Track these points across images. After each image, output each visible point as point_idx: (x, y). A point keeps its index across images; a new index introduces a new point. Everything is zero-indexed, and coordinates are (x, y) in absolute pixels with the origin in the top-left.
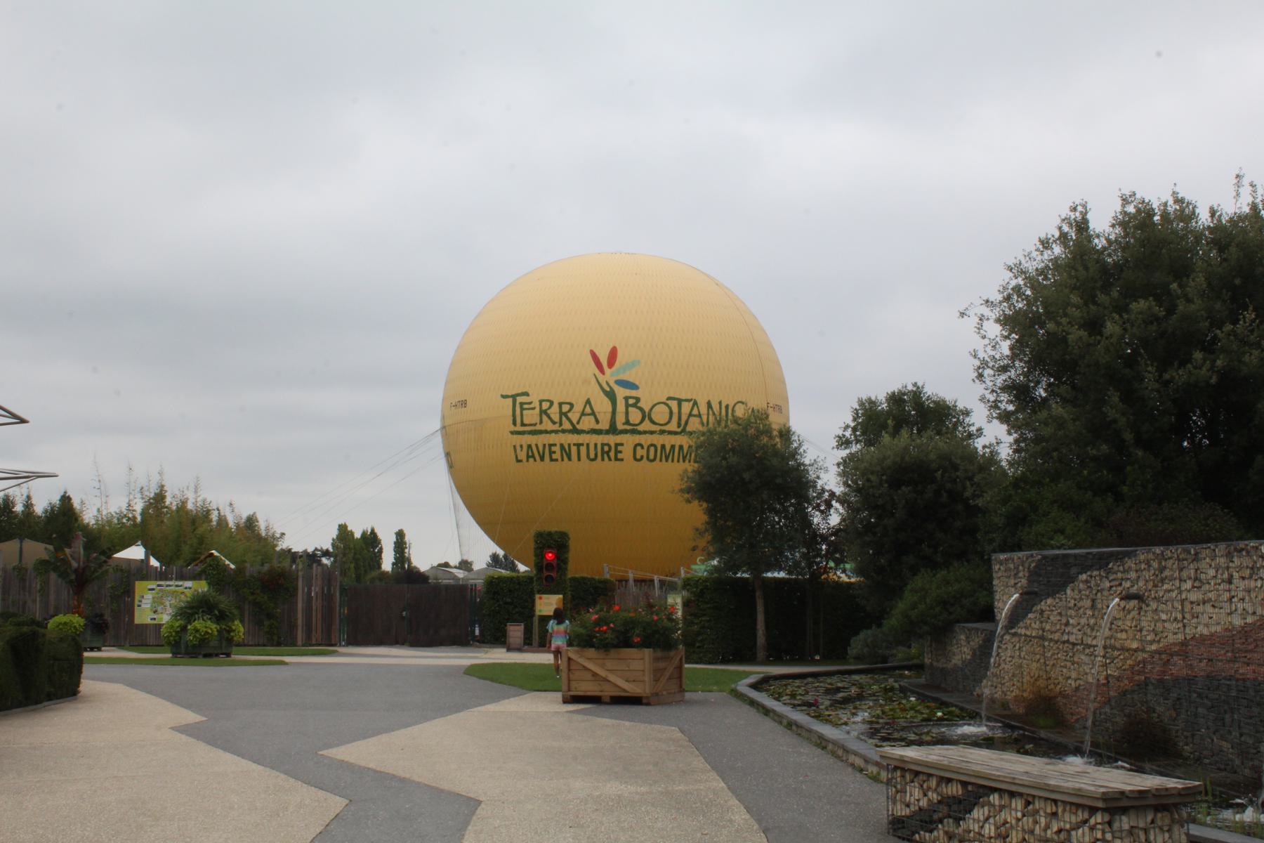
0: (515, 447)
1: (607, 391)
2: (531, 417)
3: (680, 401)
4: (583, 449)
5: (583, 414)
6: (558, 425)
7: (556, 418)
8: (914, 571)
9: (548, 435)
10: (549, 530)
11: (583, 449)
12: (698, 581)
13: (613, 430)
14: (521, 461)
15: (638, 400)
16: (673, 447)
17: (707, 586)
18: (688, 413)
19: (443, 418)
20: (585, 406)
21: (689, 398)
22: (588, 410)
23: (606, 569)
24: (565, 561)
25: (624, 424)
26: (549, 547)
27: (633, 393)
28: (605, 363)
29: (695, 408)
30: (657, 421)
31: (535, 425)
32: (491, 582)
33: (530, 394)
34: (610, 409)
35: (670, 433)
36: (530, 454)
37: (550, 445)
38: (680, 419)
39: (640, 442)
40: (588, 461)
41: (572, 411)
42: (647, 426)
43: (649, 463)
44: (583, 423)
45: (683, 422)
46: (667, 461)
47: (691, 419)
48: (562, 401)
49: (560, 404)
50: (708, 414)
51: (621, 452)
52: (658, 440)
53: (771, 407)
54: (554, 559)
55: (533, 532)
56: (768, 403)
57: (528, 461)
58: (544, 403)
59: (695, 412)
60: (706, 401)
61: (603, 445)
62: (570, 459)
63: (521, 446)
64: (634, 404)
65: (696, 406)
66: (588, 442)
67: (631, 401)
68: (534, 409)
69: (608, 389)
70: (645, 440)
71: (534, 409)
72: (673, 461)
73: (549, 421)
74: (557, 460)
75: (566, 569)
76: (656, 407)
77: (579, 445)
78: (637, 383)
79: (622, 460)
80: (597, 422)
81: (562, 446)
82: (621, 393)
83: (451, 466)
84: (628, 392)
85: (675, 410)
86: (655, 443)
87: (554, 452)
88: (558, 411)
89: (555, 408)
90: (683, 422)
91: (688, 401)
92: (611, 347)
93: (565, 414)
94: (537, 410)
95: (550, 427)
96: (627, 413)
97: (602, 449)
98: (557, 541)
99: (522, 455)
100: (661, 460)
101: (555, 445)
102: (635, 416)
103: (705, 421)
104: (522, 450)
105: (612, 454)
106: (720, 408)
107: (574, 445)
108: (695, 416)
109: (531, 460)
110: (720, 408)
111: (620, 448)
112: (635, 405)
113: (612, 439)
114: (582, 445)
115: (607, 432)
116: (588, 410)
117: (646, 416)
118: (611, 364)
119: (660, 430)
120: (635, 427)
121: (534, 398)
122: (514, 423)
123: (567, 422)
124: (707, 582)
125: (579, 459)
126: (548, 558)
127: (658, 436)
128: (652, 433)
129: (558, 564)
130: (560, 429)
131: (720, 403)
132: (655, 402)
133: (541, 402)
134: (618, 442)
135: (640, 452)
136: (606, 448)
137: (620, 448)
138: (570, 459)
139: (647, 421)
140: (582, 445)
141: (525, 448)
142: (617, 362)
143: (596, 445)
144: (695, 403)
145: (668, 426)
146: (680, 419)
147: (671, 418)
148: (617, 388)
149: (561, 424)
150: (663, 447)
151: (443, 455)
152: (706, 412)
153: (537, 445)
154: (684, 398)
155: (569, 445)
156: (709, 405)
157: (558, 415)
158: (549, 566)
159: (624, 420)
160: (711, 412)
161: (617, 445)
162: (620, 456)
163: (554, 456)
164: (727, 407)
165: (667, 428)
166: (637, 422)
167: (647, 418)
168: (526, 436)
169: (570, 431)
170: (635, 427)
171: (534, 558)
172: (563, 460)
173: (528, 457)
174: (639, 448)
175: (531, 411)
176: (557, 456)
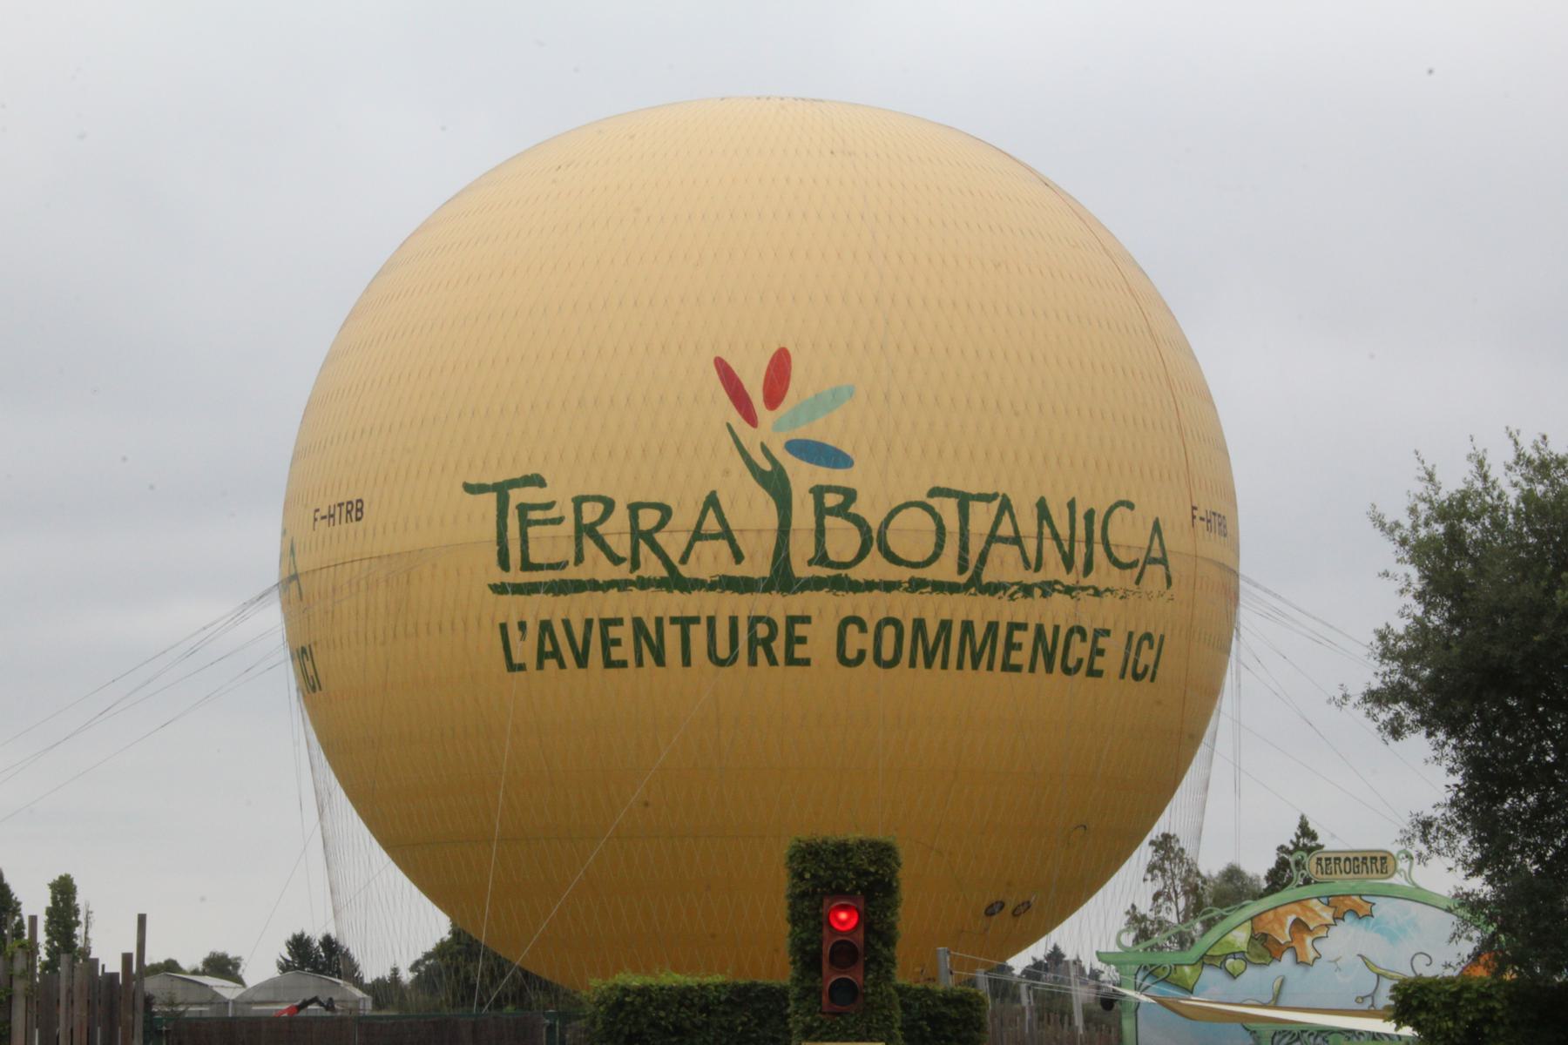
0: (504, 628)
1: (763, 472)
2: (551, 543)
3: (964, 501)
4: (698, 633)
5: (698, 535)
6: (626, 566)
7: (622, 546)
8: (1458, 977)
9: (600, 593)
10: (840, 837)
11: (698, 633)
12: (1457, 995)
13: (782, 579)
14: (522, 667)
15: (850, 495)
16: (945, 626)
17: (1493, 1010)
18: (987, 530)
19: (290, 551)
20: (704, 514)
21: (990, 491)
23: (945, 962)
24: (888, 938)
25: (810, 563)
26: (839, 892)
27: (838, 477)
28: (757, 397)
29: (1006, 518)
30: (901, 555)
32: (620, 1004)
34: (771, 519)
35: (939, 587)
36: (548, 647)
37: (606, 623)
38: (964, 547)
39: (858, 614)
40: (710, 666)
41: (667, 528)
42: (874, 567)
43: (881, 671)
44: (698, 558)
45: (973, 557)
46: (928, 664)
47: (997, 549)
48: (637, 499)
49: (634, 509)
51: (802, 640)
52: (905, 606)
53: (1202, 519)
54: (856, 928)
55: (782, 851)
56: (1194, 508)
57: (540, 666)
58: (586, 507)
59: (1006, 529)
61: (754, 621)
62: (660, 660)
63: (522, 626)
64: (839, 506)
65: (1007, 514)
66: (712, 614)
67: (831, 500)
68: (558, 521)
69: (767, 466)
70: (870, 606)
71: (558, 521)
72: (944, 665)
73: (603, 557)
74: (623, 664)
75: (891, 961)
77: (685, 623)
78: (847, 449)
79: (806, 662)
80: (738, 556)
81: (638, 624)
82: (803, 477)
83: (311, 684)
84: (824, 476)
86: (897, 615)
87: (617, 642)
88: (626, 525)
89: (620, 518)
90: (973, 557)
91: (987, 498)
92: (774, 348)
93: (648, 537)
94: (568, 527)
95: (604, 570)
96: (820, 531)
97: (752, 627)
98: (869, 873)
99: (525, 650)
100: (913, 664)
101: (618, 622)
102: (842, 540)
103: (1032, 554)
104: (523, 638)
107: (674, 620)
108: (1004, 540)
109: (551, 664)
111: (800, 630)
112: (841, 511)
113: (778, 606)
114: (696, 620)
115: (768, 586)
116: (711, 524)
117: (872, 540)
118: (774, 396)
119: (911, 581)
120: (843, 572)
121: (560, 492)
122: (504, 563)
123: (654, 557)
124: (1490, 997)
125: (687, 662)
126: (837, 926)
127: (907, 594)
128: (889, 586)
129: (867, 942)
130: (633, 577)
131: (1072, 505)
132: (901, 501)
133: (579, 502)
134: (796, 612)
135: (857, 641)
136: (762, 631)
137: (800, 630)
138: (660, 660)
140: (696, 620)
142: (792, 385)
143: (733, 621)
144: (1006, 506)
145: (934, 566)
146: (964, 547)
147: (940, 545)
148: (790, 463)
149: (635, 564)
150: (919, 625)
151: (284, 654)
152: (1034, 530)
153: (567, 624)
154: (973, 488)
155: (659, 621)
157: (627, 539)
158: (845, 953)
159: (811, 552)
160: (1047, 531)
161: (792, 621)
162: (800, 651)
163: (616, 654)
164: (1090, 515)
165: (928, 574)
166: (848, 556)
169: (661, 584)
170: (843, 572)
171: (789, 927)
172: (640, 663)
173: (542, 656)
174: (852, 629)
175: (549, 530)
176: (623, 652)
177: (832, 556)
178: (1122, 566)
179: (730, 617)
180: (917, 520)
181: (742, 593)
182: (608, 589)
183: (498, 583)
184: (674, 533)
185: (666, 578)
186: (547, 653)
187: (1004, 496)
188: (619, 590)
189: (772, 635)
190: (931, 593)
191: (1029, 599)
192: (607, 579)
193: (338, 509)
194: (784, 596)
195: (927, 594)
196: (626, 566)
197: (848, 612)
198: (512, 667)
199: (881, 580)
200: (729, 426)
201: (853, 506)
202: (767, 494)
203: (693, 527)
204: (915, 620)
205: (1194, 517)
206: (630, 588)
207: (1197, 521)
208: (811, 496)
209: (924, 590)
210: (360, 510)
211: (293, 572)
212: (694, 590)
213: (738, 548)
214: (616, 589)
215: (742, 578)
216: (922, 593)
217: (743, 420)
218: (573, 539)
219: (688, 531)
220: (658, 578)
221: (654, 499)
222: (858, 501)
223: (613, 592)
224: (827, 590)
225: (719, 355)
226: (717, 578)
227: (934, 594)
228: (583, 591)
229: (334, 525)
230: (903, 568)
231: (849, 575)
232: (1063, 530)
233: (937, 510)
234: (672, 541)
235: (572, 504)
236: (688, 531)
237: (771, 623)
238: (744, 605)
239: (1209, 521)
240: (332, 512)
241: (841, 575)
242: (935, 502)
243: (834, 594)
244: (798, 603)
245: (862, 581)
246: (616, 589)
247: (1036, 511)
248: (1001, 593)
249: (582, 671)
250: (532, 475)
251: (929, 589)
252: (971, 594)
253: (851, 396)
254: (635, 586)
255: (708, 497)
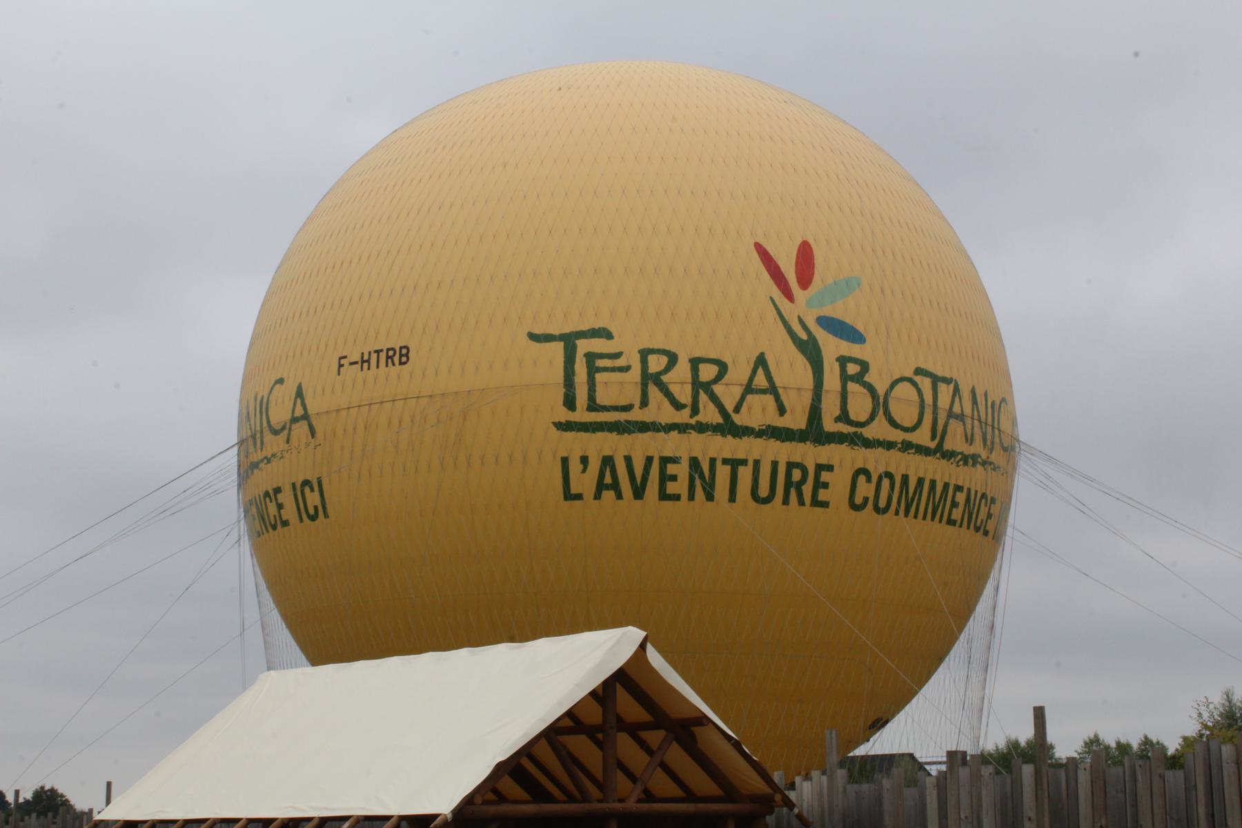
0: (565, 461)
1: (801, 340)
3: (936, 380)
4: (745, 474)
5: (749, 389)
6: (686, 412)
7: (685, 396)
9: (662, 434)
11: (745, 474)
13: (814, 433)
14: (579, 497)
20: (754, 372)
22: (761, 380)
25: (838, 420)
30: (899, 421)
31: (628, 408)
33: (615, 334)
34: (808, 381)
36: (608, 479)
37: (665, 461)
39: (867, 467)
41: (723, 381)
44: (749, 409)
46: (906, 515)
48: (697, 354)
49: (695, 363)
51: (826, 485)
52: (900, 463)
57: (598, 496)
58: (652, 359)
61: (791, 466)
62: (710, 497)
63: (584, 460)
67: (852, 369)
68: (627, 369)
69: (804, 336)
70: (876, 460)
71: (627, 369)
72: (916, 517)
73: (666, 402)
74: (677, 497)
77: (735, 464)
78: (860, 328)
79: (825, 505)
80: (782, 410)
81: (694, 463)
82: (832, 347)
85: (928, 399)
86: (892, 470)
87: (674, 478)
89: (682, 371)
92: (799, 241)
94: (635, 374)
95: (668, 415)
99: (584, 482)
100: (897, 513)
101: (675, 460)
102: (860, 406)
104: (584, 471)
105: (807, 489)
107: (725, 462)
109: (609, 495)
111: (825, 476)
112: (859, 378)
113: (810, 454)
116: (761, 380)
117: (880, 404)
118: (805, 282)
119: (903, 442)
121: (628, 343)
122: (570, 403)
123: (711, 406)
125: (732, 498)
127: (900, 453)
128: (889, 445)
130: (693, 421)
132: (897, 376)
133: (645, 354)
134: (823, 461)
135: (865, 489)
137: (825, 476)
138: (710, 497)
139: (880, 418)
140: (744, 462)
141: (594, 465)
143: (775, 465)
144: (956, 390)
148: (822, 336)
149: (695, 411)
150: (905, 478)
153: (628, 460)
157: (689, 388)
159: (837, 413)
161: (820, 468)
162: (823, 495)
163: (671, 488)
164: (993, 404)
165: (914, 438)
166: (863, 418)
167: (881, 412)
168: (600, 435)
169: (717, 429)
170: (859, 430)
172: (691, 497)
173: (600, 487)
174: (862, 479)
176: (678, 487)
177: (852, 416)
179: (772, 462)
180: (904, 390)
181: (783, 441)
182: (669, 431)
183: (563, 421)
184: (730, 387)
185: (721, 424)
186: (607, 484)
188: (679, 433)
189: (803, 480)
190: (914, 454)
191: (966, 467)
192: (670, 422)
193: (374, 356)
194: (815, 446)
195: (912, 455)
196: (686, 412)
197: (859, 465)
198: (569, 496)
199: (884, 440)
200: (771, 298)
201: (867, 375)
202: (804, 359)
203: (745, 382)
204: (903, 475)
206: (687, 431)
208: (838, 363)
209: (910, 451)
210: (407, 355)
211: (299, 412)
212: (744, 436)
213: (782, 403)
214: (676, 432)
215: (784, 428)
216: (909, 453)
217: (783, 296)
218: (640, 386)
219: (742, 385)
220: (714, 424)
221: (713, 356)
222: (870, 371)
223: (674, 434)
224: (847, 444)
225: (758, 241)
226: (764, 427)
227: (916, 455)
228: (646, 432)
229: (369, 369)
230: (898, 431)
231: (863, 433)
233: (920, 386)
234: (728, 394)
235: (639, 355)
236: (742, 385)
237: (805, 471)
238: (784, 452)
240: (366, 358)
241: (857, 432)
242: (918, 379)
243: (852, 448)
244: (826, 453)
245: (871, 439)
246: (676, 432)
248: (952, 460)
249: (639, 502)
250: (599, 328)
251: (913, 451)
252: (937, 458)
253: (859, 285)
254: (695, 431)
255: (758, 357)
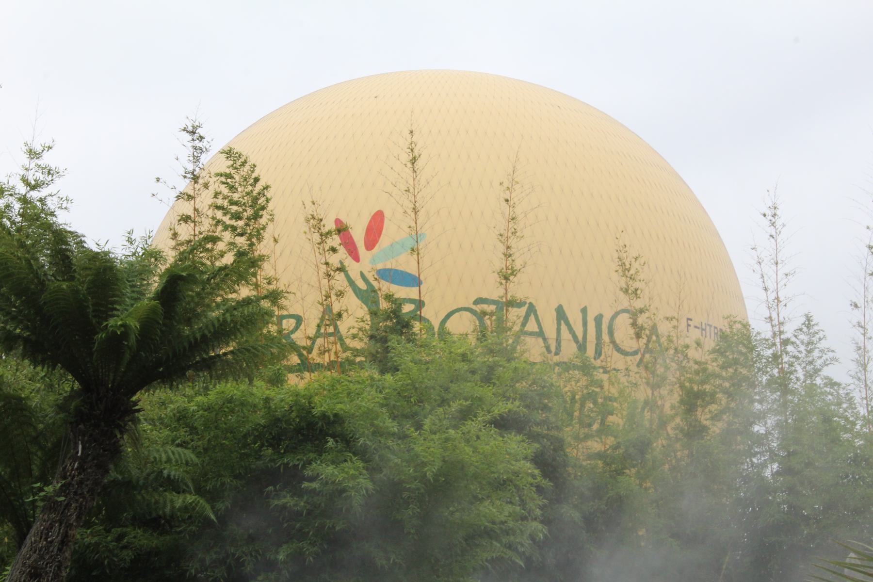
50: (559, 330)
53: (696, 327)
60: (556, 306)
65: (532, 317)
76: (452, 318)
106: (585, 324)
108: (532, 334)
110: (585, 324)
131: (584, 311)
144: (532, 309)
156: (561, 315)
164: (599, 319)
178: (625, 353)
187: (531, 304)
205: (689, 325)
207: (691, 329)
232: (579, 332)
239: (703, 330)
247: (555, 314)
